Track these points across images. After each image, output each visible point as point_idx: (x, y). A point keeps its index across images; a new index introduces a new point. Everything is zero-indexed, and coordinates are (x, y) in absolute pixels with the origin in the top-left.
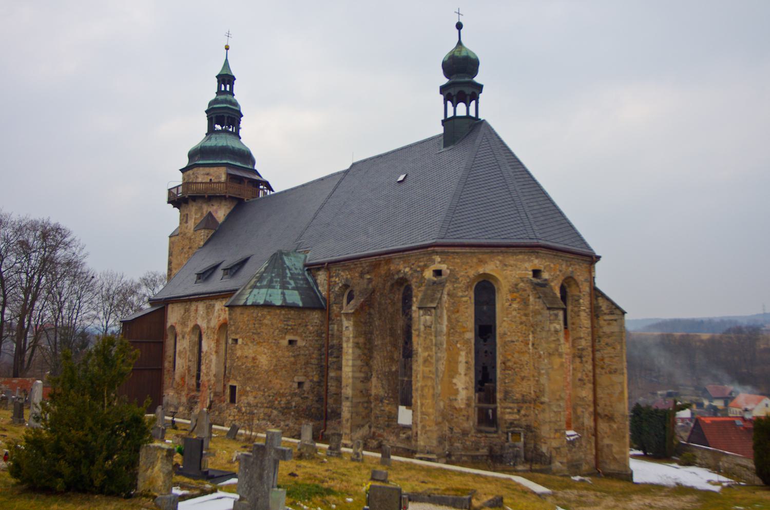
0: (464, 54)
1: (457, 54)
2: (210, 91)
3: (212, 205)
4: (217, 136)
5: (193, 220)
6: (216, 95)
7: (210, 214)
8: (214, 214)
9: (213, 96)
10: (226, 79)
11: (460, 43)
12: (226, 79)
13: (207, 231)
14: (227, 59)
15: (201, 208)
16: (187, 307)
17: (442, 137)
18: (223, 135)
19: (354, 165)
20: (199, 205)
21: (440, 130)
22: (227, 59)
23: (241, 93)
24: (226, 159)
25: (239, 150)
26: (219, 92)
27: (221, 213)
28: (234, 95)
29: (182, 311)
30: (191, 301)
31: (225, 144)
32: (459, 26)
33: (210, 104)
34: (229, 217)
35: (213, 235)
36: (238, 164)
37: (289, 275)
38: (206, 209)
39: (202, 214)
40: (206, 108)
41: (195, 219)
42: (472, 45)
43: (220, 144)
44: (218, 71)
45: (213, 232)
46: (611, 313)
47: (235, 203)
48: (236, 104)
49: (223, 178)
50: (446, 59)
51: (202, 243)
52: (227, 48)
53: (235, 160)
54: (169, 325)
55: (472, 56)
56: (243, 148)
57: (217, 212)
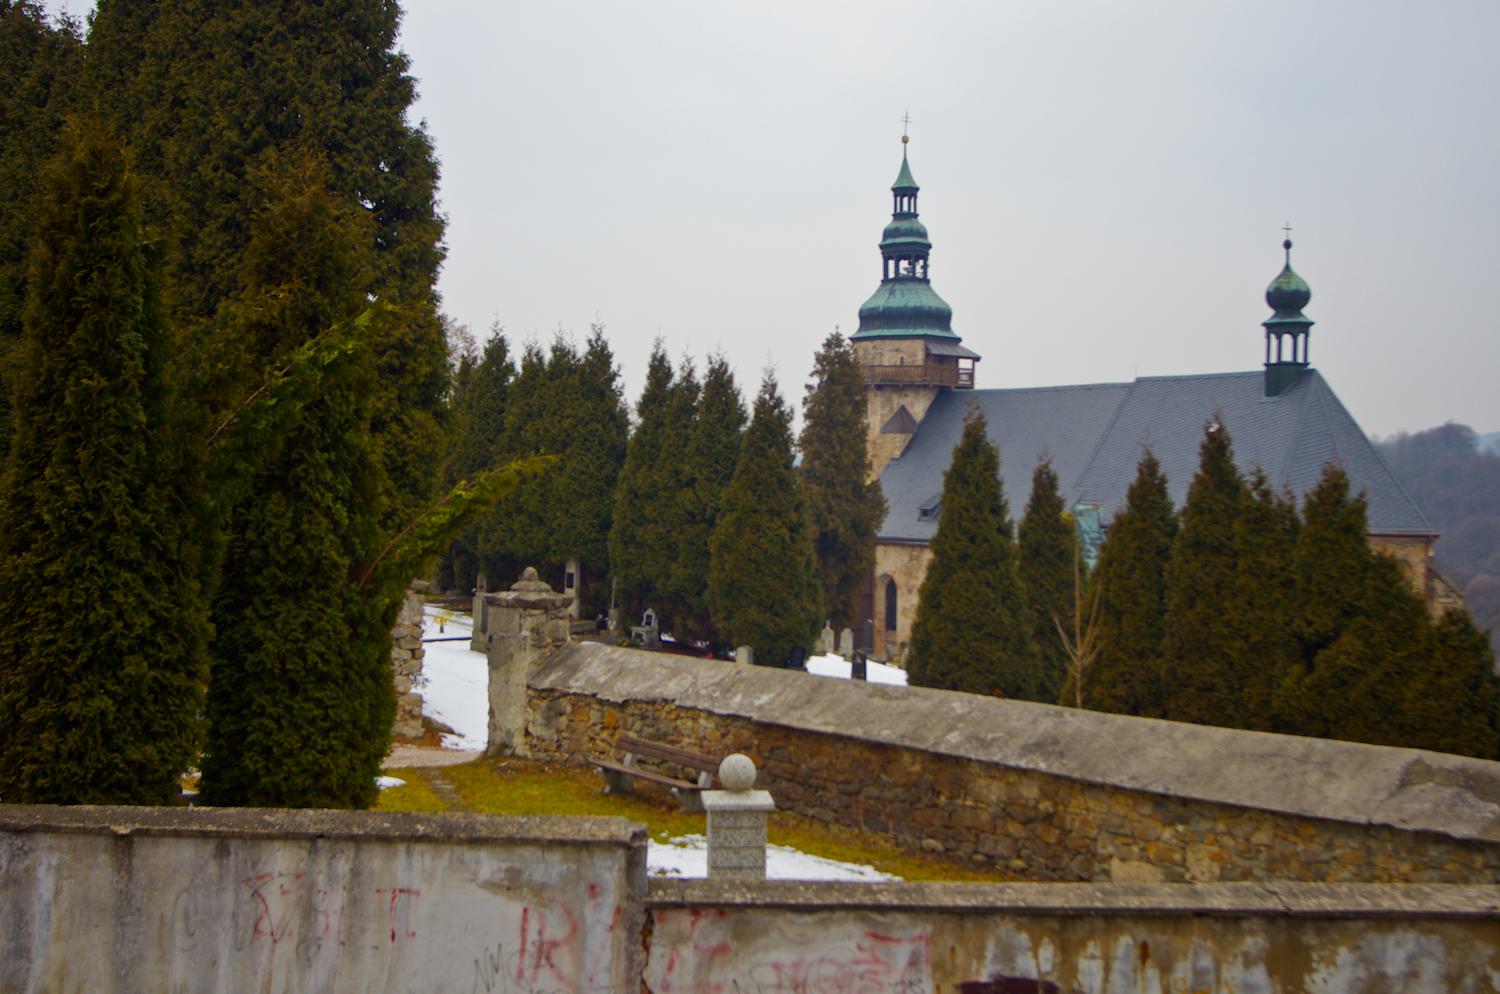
0: (1293, 287)
1: (1285, 287)
2: (881, 214)
3: (906, 396)
4: (903, 287)
5: (879, 417)
6: (892, 218)
7: (903, 409)
8: (908, 408)
9: (887, 220)
10: (906, 191)
11: (1287, 268)
12: (906, 191)
13: (903, 436)
14: (905, 160)
15: (889, 400)
16: (915, 553)
17: (1262, 379)
18: (911, 286)
19: (1139, 381)
20: (887, 395)
21: (1263, 369)
22: (905, 160)
23: (929, 213)
24: (922, 327)
25: (937, 309)
26: (897, 216)
27: (918, 407)
28: (915, 216)
29: (906, 559)
30: (921, 547)
31: (919, 305)
32: (1288, 245)
33: (887, 234)
34: (931, 412)
35: (912, 441)
36: (937, 332)
37: (1088, 541)
38: (897, 401)
39: (892, 408)
40: (879, 239)
41: (882, 416)
42: (1306, 272)
43: (912, 304)
44: (892, 179)
45: (911, 435)
46: (1447, 596)
47: (936, 392)
48: (924, 235)
49: (920, 356)
50: (1271, 290)
51: (897, 453)
52: (905, 140)
53: (931, 326)
54: (880, 571)
55: (1303, 289)
56: (943, 307)
57: (912, 406)
